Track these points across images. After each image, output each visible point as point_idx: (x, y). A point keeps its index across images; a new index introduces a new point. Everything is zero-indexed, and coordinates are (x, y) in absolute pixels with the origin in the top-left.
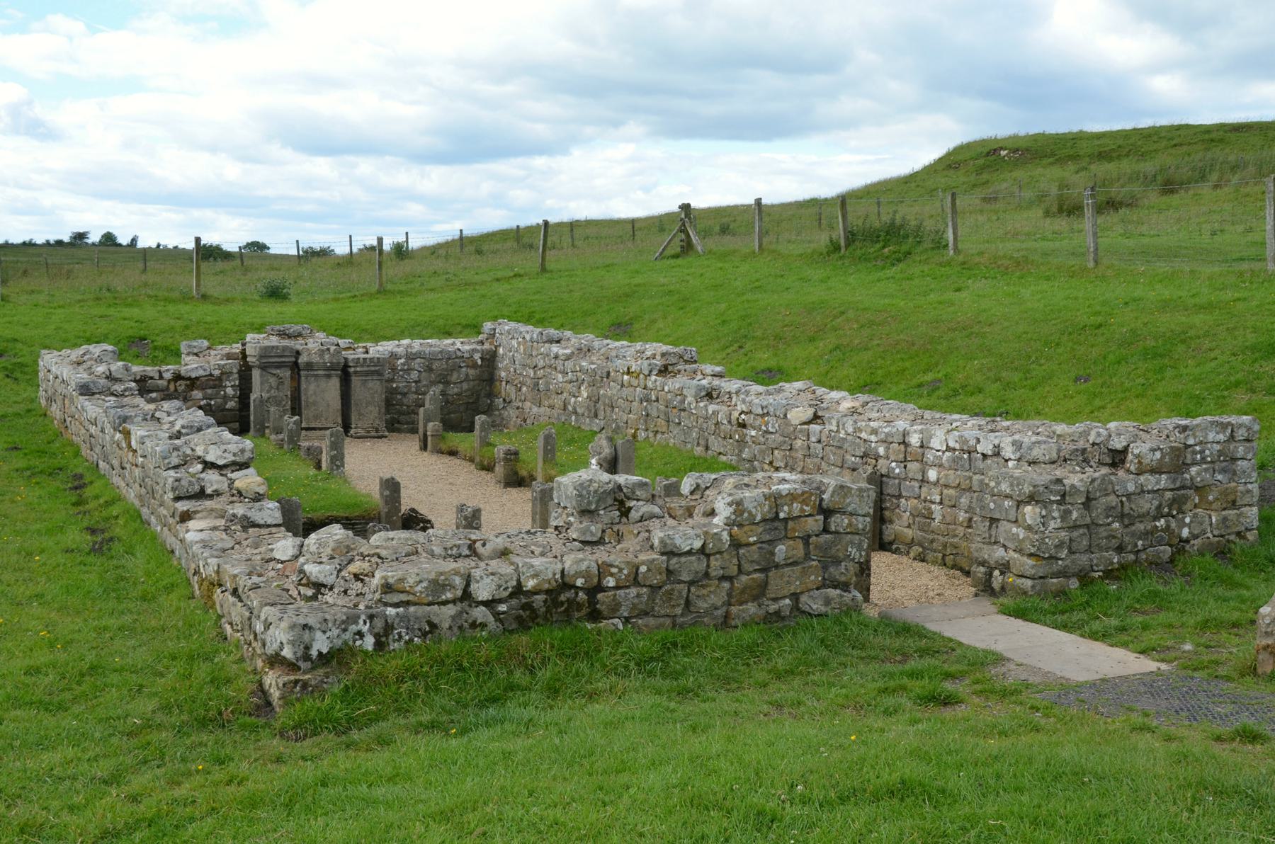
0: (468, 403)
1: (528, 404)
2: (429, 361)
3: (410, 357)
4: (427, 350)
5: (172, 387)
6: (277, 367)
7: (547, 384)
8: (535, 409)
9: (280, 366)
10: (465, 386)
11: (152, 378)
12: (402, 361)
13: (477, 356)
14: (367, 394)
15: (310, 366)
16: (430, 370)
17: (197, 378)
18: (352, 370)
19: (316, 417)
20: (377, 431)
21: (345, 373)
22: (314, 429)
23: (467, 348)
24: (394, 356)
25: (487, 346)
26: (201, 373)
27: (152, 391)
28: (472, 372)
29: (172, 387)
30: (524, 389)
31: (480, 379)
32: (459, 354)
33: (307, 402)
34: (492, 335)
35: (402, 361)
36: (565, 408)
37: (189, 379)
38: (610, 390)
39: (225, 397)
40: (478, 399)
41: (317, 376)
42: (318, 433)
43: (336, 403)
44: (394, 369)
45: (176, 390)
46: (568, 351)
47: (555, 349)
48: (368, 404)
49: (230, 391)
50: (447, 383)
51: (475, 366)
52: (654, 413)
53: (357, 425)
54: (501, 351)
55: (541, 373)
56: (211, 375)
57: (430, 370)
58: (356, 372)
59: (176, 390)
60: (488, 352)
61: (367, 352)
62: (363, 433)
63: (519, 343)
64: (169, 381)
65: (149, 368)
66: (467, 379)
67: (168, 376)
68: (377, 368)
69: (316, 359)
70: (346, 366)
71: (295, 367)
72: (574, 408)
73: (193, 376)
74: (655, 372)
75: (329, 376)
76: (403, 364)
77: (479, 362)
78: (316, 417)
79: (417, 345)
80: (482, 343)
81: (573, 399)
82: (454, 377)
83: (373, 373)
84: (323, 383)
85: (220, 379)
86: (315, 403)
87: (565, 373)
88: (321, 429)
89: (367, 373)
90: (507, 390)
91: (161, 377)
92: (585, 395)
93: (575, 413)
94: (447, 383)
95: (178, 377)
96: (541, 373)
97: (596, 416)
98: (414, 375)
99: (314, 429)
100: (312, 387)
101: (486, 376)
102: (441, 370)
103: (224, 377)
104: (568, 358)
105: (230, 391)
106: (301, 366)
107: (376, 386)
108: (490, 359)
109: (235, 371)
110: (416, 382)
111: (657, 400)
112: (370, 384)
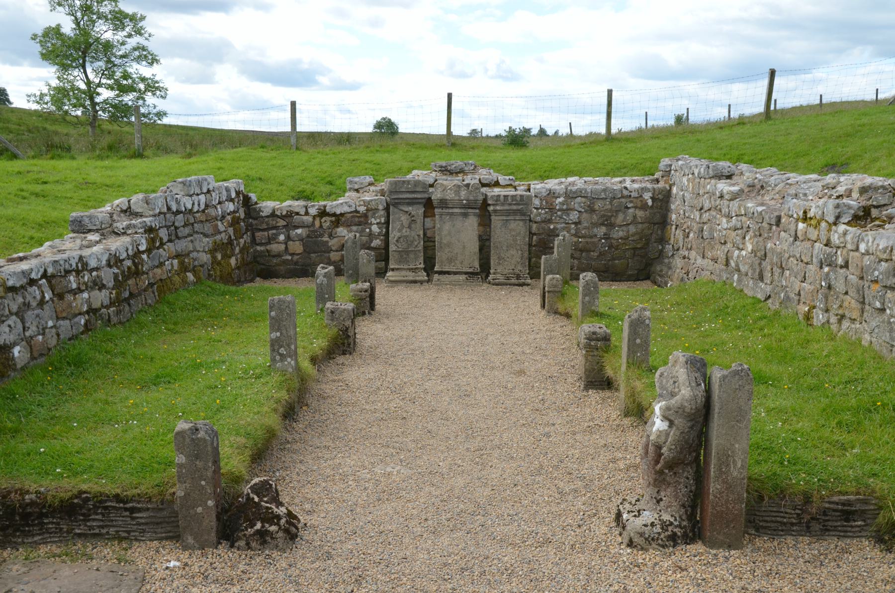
0: (635, 249)
1: (693, 254)
2: (591, 200)
3: (570, 195)
4: (589, 188)
5: (317, 223)
6: (409, 204)
7: (711, 230)
8: (700, 261)
9: (412, 202)
10: (632, 229)
11: (297, 214)
12: (561, 199)
13: (647, 196)
14: (509, 237)
15: (444, 203)
16: (591, 210)
17: (342, 215)
18: (491, 208)
19: (450, 260)
20: (518, 277)
21: (483, 210)
22: (448, 273)
23: (636, 186)
24: (552, 194)
25: (661, 185)
26: (346, 209)
27: (297, 227)
28: (640, 214)
29: (317, 223)
30: (691, 235)
31: (650, 222)
32: (625, 193)
33: (440, 243)
34: (667, 173)
35: (561, 199)
36: (727, 264)
37: (334, 215)
38: (781, 243)
39: (371, 235)
40: (647, 244)
41: (452, 214)
42: (457, 277)
43: (473, 246)
44: (552, 209)
45: (321, 226)
46: (736, 188)
47: (723, 186)
48: (509, 247)
49: (375, 229)
50: (611, 226)
51: (644, 207)
52: (840, 286)
53: (498, 270)
54: (674, 190)
55: (706, 216)
56: (356, 211)
57: (591, 210)
58: (495, 211)
59: (321, 226)
60: (661, 191)
61: (529, 190)
62: (502, 279)
63: (688, 180)
64: (314, 217)
65: (296, 203)
66: (634, 221)
67: (313, 211)
68: (519, 208)
69: (450, 195)
70: (485, 203)
71: (428, 204)
72: (737, 265)
73: (338, 212)
74: (846, 218)
75: (465, 215)
76: (562, 204)
77: (650, 203)
78: (450, 260)
79: (577, 182)
80: (657, 181)
81: (737, 252)
82: (621, 217)
83: (515, 212)
84: (459, 222)
85: (365, 216)
86: (449, 245)
87: (729, 217)
88: (455, 273)
89: (508, 213)
90: (675, 235)
91: (307, 213)
92: (750, 247)
93: (738, 270)
94: (611, 226)
95: (323, 213)
96: (706, 216)
97: (761, 278)
98: (574, 216)
99: (448, 273)
100: (447, 227)
101: (657, 218)
102: (605, 209)
103: (370, 214)
104: (734, 197)
105: (375, 229)
106: (435, 203)
107: (518, 226)
108: (663, 199)
109: (381, 207)
110: (576, 223)
111: (846, 265)
112: (513, 225)
